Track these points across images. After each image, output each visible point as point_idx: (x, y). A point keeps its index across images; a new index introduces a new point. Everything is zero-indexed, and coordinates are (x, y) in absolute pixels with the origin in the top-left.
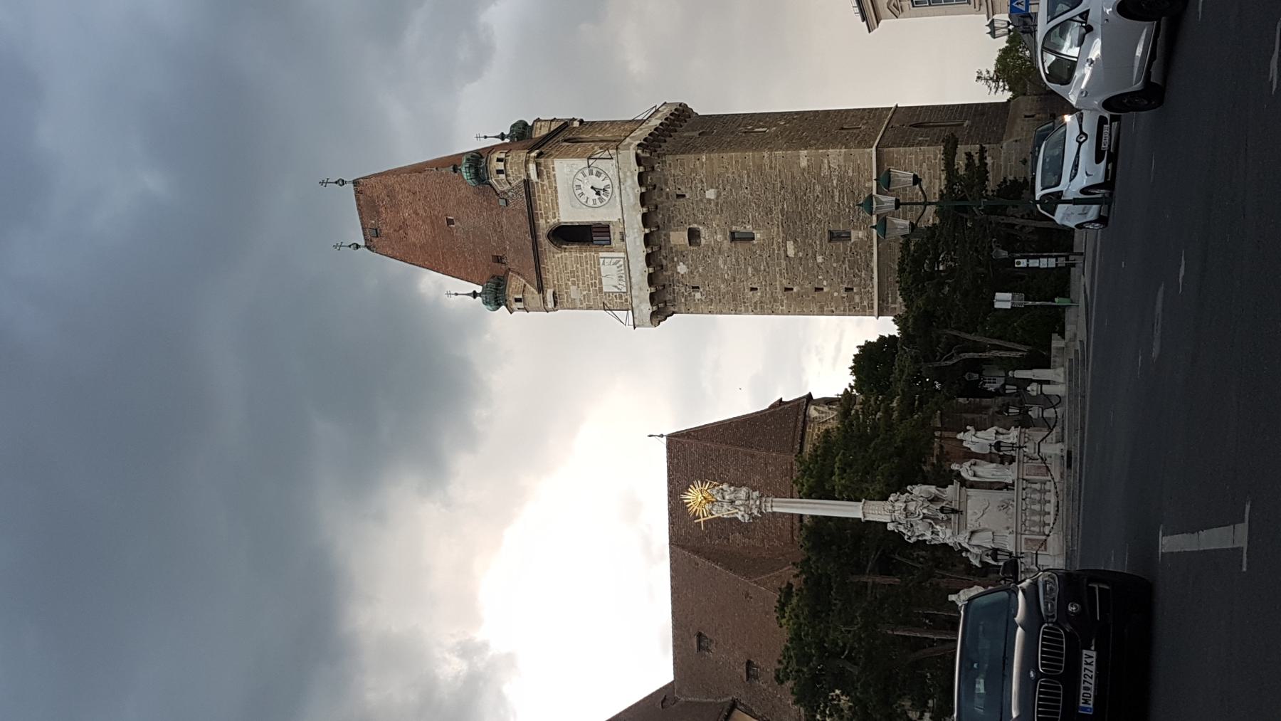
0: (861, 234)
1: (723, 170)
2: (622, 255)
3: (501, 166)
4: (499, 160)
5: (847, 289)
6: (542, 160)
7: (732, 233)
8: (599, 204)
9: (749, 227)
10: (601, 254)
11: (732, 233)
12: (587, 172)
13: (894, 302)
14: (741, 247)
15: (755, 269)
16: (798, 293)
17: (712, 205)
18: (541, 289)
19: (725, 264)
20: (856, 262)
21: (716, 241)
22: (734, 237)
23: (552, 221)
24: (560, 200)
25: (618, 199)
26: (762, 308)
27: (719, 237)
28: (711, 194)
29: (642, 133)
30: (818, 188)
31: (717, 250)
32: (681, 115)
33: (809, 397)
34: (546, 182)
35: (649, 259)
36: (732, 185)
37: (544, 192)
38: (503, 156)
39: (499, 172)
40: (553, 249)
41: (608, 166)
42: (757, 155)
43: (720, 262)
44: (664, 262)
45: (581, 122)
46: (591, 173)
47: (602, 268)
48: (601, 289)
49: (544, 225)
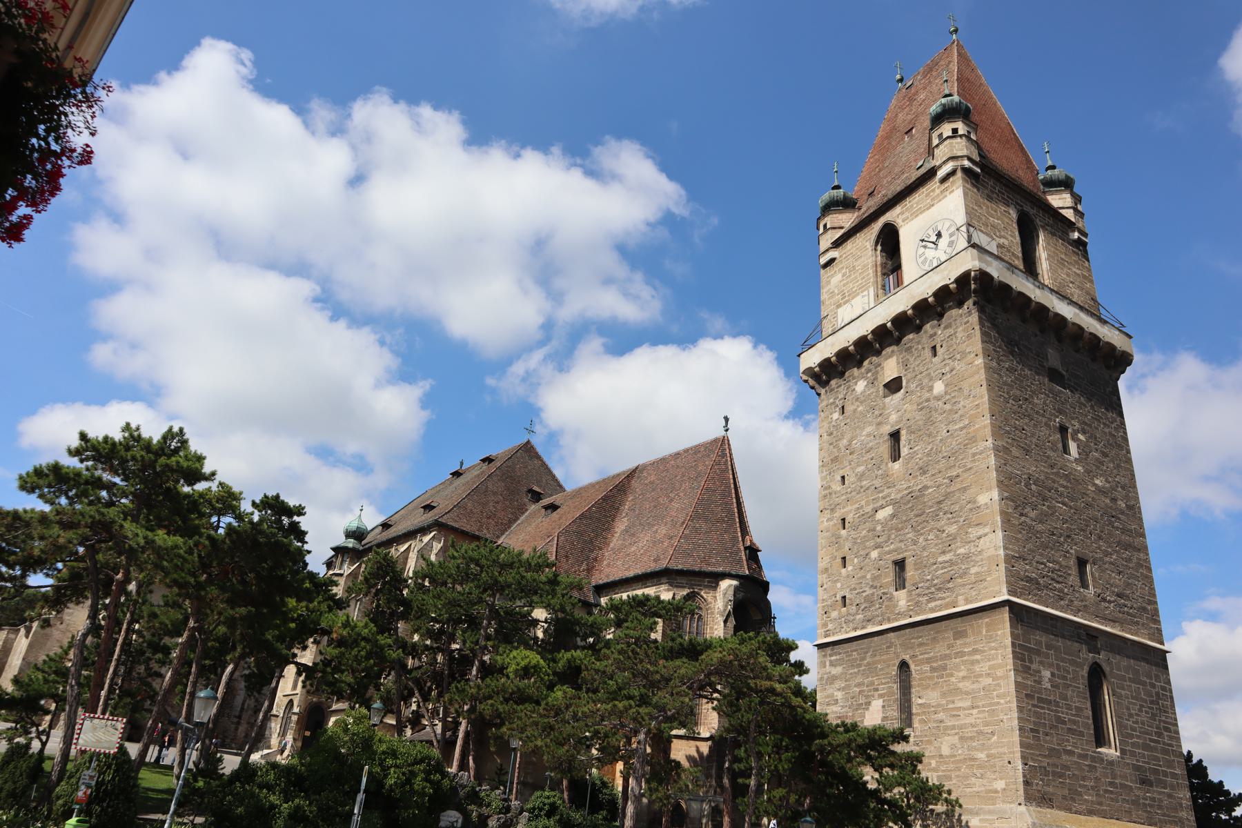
1: (966, 392)
4: (955, 131)
5: (844, 597)
6: (959, 174)
8: (920, 260)
9: (904, 451)
10: (872, 290)
12: (953, 229)
13: (832, 664)
14: (885, 448)
15: (863, 474)
16: (839, 537)
17: (927, 395)
18: (837, 244)
19: (868, 435)
21: (889, 414)
22: (895, 436)
23: (899, 222)
24: (921, 217)
26: (825, 496)
27: (894, 417)
28: (939, 387)
30: (952, 529)
34: (938, 191)
38: (960, 132)
42: (988, 431)
43: (869, 429)
44: (866, 363)
46: (951, 235)
48: (839, 306)
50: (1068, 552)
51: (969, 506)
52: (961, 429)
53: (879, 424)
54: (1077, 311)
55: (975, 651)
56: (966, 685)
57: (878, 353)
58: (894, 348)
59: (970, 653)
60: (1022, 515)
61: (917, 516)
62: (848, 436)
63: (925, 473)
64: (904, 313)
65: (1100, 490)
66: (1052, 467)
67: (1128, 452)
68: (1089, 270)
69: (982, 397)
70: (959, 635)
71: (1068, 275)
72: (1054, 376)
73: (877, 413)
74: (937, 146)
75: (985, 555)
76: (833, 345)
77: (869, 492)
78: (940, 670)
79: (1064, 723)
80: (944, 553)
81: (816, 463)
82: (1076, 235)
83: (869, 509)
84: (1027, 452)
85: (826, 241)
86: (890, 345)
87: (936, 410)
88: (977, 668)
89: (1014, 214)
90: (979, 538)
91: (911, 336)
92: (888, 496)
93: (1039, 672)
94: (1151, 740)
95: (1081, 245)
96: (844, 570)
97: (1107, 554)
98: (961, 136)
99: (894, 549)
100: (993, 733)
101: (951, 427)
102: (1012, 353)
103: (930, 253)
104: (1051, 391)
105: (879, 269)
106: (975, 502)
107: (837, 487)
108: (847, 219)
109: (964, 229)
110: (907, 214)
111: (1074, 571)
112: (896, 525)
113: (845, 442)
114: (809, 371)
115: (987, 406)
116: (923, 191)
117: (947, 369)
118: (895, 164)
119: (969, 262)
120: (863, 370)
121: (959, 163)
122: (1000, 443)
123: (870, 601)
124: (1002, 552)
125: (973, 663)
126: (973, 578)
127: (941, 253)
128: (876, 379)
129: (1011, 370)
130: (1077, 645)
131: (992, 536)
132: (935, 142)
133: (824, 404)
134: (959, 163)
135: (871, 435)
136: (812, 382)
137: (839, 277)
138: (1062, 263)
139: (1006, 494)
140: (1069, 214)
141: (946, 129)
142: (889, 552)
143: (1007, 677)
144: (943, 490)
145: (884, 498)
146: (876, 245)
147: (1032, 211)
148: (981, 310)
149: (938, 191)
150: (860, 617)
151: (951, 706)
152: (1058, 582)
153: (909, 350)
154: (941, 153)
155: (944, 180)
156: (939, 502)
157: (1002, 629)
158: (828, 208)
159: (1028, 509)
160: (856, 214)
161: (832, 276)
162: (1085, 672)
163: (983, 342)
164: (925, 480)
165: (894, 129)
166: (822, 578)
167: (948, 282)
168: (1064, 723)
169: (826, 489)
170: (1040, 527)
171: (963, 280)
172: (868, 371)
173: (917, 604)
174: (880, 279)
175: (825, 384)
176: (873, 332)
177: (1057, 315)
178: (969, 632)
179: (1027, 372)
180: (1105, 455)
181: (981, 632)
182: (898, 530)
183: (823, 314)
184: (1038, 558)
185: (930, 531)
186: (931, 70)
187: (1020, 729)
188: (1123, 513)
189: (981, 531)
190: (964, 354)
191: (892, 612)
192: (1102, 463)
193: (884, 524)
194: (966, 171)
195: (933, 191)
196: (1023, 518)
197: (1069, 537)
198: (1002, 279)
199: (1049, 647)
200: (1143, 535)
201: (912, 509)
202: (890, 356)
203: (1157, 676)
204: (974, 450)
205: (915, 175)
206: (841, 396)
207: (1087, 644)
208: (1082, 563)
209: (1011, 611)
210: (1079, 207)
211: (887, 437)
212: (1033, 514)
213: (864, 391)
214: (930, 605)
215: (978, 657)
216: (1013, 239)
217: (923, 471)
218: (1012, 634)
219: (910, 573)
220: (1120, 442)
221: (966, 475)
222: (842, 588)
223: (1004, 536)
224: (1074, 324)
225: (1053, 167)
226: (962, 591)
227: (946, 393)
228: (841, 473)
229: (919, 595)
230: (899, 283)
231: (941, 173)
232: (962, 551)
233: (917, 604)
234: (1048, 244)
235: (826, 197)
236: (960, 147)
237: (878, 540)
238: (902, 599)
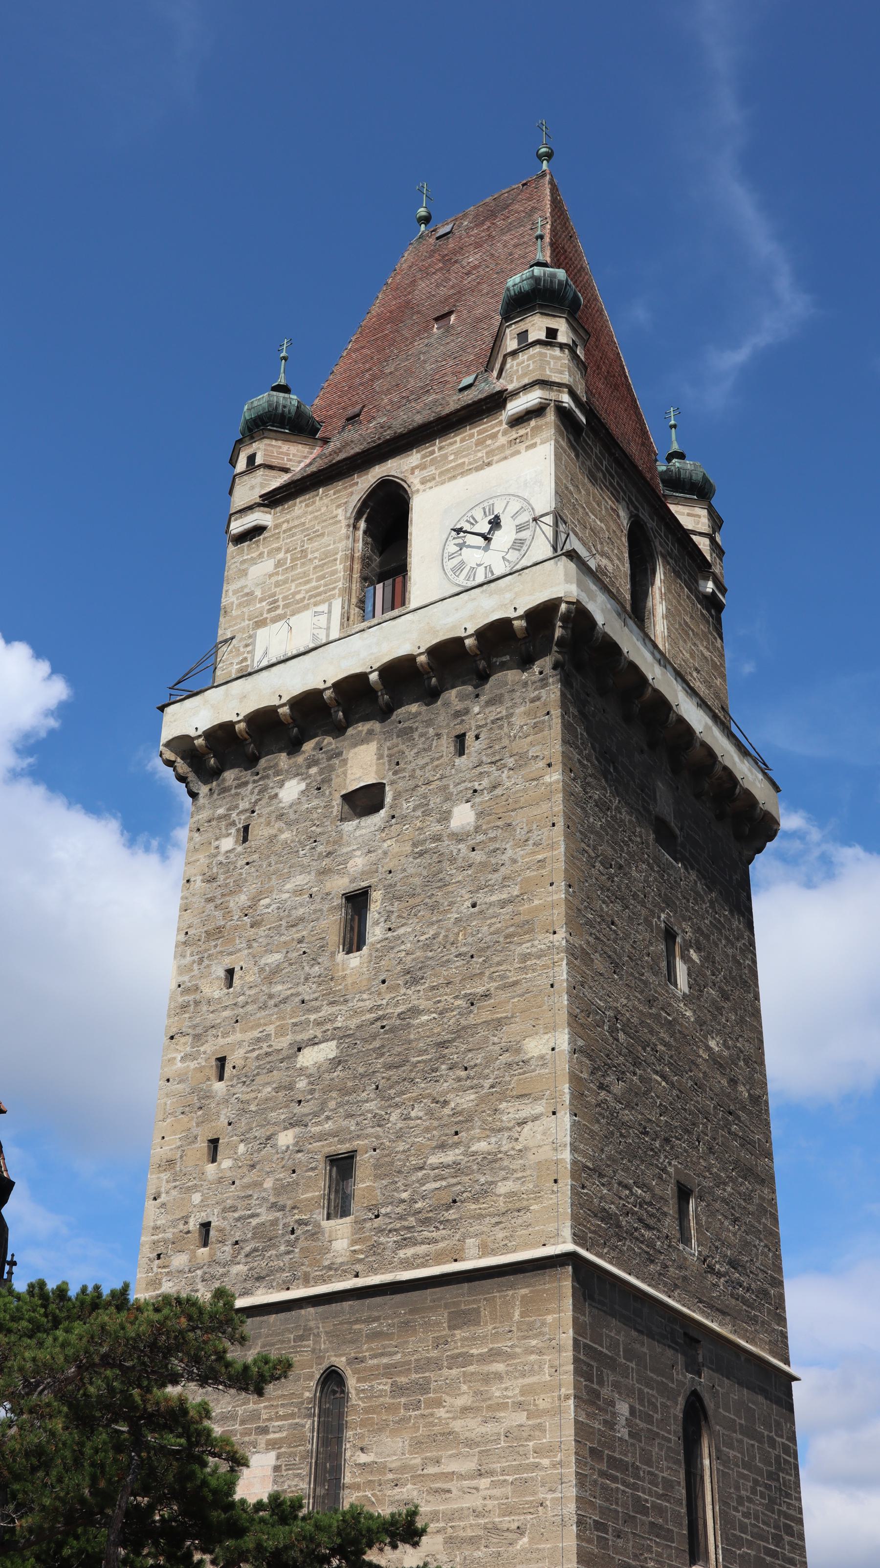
1: (520, 834)
4: (552, 333)
6: (551, 416)
8: (450, 564)
9: (375, 933)
12: (526, 517)
14: (332, 923)
15: (276, 970)
16: (208, 1095)
17: (436, 828)
18: (273, 500)
19: (298, 892)
20: (271, 1241)
21: (350, 856)
22: (357, 902)
23: (414, 482)
24: (461, 482)
26: (184, 1007)
27: (358, 863)
28: (463, 816)
30: (467, 1100)
31: (331, 860)
34: (502, 440)
36: (483, 865)
37: (478, 444)
42: (559, 915)
43: (300, 880)
44: (308, 747)
46: (520, 528)
47: (306, 615)
48: (261, 623)
50: (664, 1170)
51: (506, 1058)
52: (503, 904)
53: (324, 872)
54: (710, 722)
55: (494, 1355)
56: (470, 1427)
57: (339, 730)
58: (375, 725)
59: (483, 1359)
60: (601, 1087)
61: (389, 1067)
62: (251, 888)
63: (415, 981)
64: (410, 659)
65: (716, 1062)
66: (650, 1002)
67: (757, 997)
68: (722, 656)
69: (552, 847)
70: (463, 1318)
71: (692, 655)
72: (664, 835)
73: (321, 848)
74: (514, 353)
75: (532, 1159)
76: (244, 697)
77: (288, 1007)
78: (415, 1391)
79: (644, 1511)
80: (442, 1147)
81: (171, 938)
82: (710, 587)
83: (283, 1043)
84: (617, 967)
85: (249, 490)
86: (366, 718)
87: (453, 860)
88: (496, 1391)
89: (625, 522)
90: (522, 1123)
91: (414, 708)
92: (331, 1019)
93: (612, 1404)
94: (768, 1552)
95: (713, 605)
96: (211, 1168)
97: (720, 1183)
98: (562, 346)
99: (332, 1130)
100: (520, 1531)
101: (481, 898)
102: (605, 774)
103: (473, 556)
104: (657, 860)
105: (357, 566)
106: (518, 1051)
107: (214, 990)
108: (298, 457)
109: (549, 519)
110: (432, 470)
111: (671, 1209)
112: (341, 1082)
113: (243, 899)
114: (183, 746)
115: (561, 865)
116: (471, 434)
117: (485, 782)
118: (409, 372)
119: (558, 583)
120: (300, 759)
121: (552, 395)
122: (577, 941)
123: (265, 1236)
124: (566, 1155)
125: (487, 1379)
126: (501, 1205)
127: (496, 557)
128: (327, 781)
129: (602, 806)
130: (669, 1353)
131: (549, 1122)
132: (511, 344)
133: (204, 815)
134: (552, 395)
135: (303, 892)
136: (182, 767)
137: (268, 565)
138: (684, 629)
139: (581, 1043)
140: (703, 544)
141: (537, 326)
142: (321, 1137)
143: (559, 1411)
144: (451, 1019)
145: (318, 1023)
146: (358, 517)
147: (651, 524)
148: (566, 682)
149: (502, 440)
150: (239, 1269)
151: (431, 1470)
152: (648, 1227)
153: (406, 733)
154: (519, 369)
155: (518, 421)
156: (443, 1045)
157: (557, 1313)
158: (264, 424)
159: (611, 1078)
160: (317, 451)
161: (253, 561)
162: (678, 1410)
163: (565, 742)
164: (416, 997)
165: (405, 308)
166: (156, 1180)
167: (513, 615)
168: (644, 1511)
169: (187, 991)
170: (627, 1115)
171: (542, 615)
172: (312, 762)
173: (374, 1249)
174: (356, 586)
175: (209, 775)
176: (337, 686)
177: (681, 721)
178: (485, 1313)
179: (625, 816)
180: (725, 997)
181: (510, 1316)
182: (344, 1091)
183: (223, 633)
184: (621, 1175)
185: (417, 1100)
186: (492, 214)
187: (579, 1523)
188: (743, 1108)
189: (527, 1110)
190: (523, 759)
191: (315, 1263)
192: (720, 1009)
193: (315, 1077)
194: (563, 413)
195: (494, 436)
196: (603, 1093)
197: (667, 1140)
198: (607, 629)
199: (630, 1354)
200: (769, 1155)
201: (380, 1052)
202: (364, 741)
203: (778, 1424)
204: (525, 948)
205: (454, 402)
206: (244, 805)
207: (684, 1354)
208: (684, 1194)
209: (576, 1277)
210: (718, 539)
211: (338, 901)
212: (618, 1088)
213: (298, 802)
214: (402, 1254)
215: (500, 1367)
216: (618, 566)
217: (413, 977)
218: (575, 1320)
219: (364, 1183)
220: (748, 980)
221: (503, 995)
222: (203, 1205)
223: (574, 1124)
224: (704, 745)
225: (681, 456)
226: (476, 1228)
227: (477, 829)
229: (380, 1231)
230: (397, 600)
231: (515, 407)
232: (482, 1146)
233: (374, 1249)
234: (668, 589)
235: (262, 400)
236: (557, 365)
237: (297, 1109)
238: (340, 1236)
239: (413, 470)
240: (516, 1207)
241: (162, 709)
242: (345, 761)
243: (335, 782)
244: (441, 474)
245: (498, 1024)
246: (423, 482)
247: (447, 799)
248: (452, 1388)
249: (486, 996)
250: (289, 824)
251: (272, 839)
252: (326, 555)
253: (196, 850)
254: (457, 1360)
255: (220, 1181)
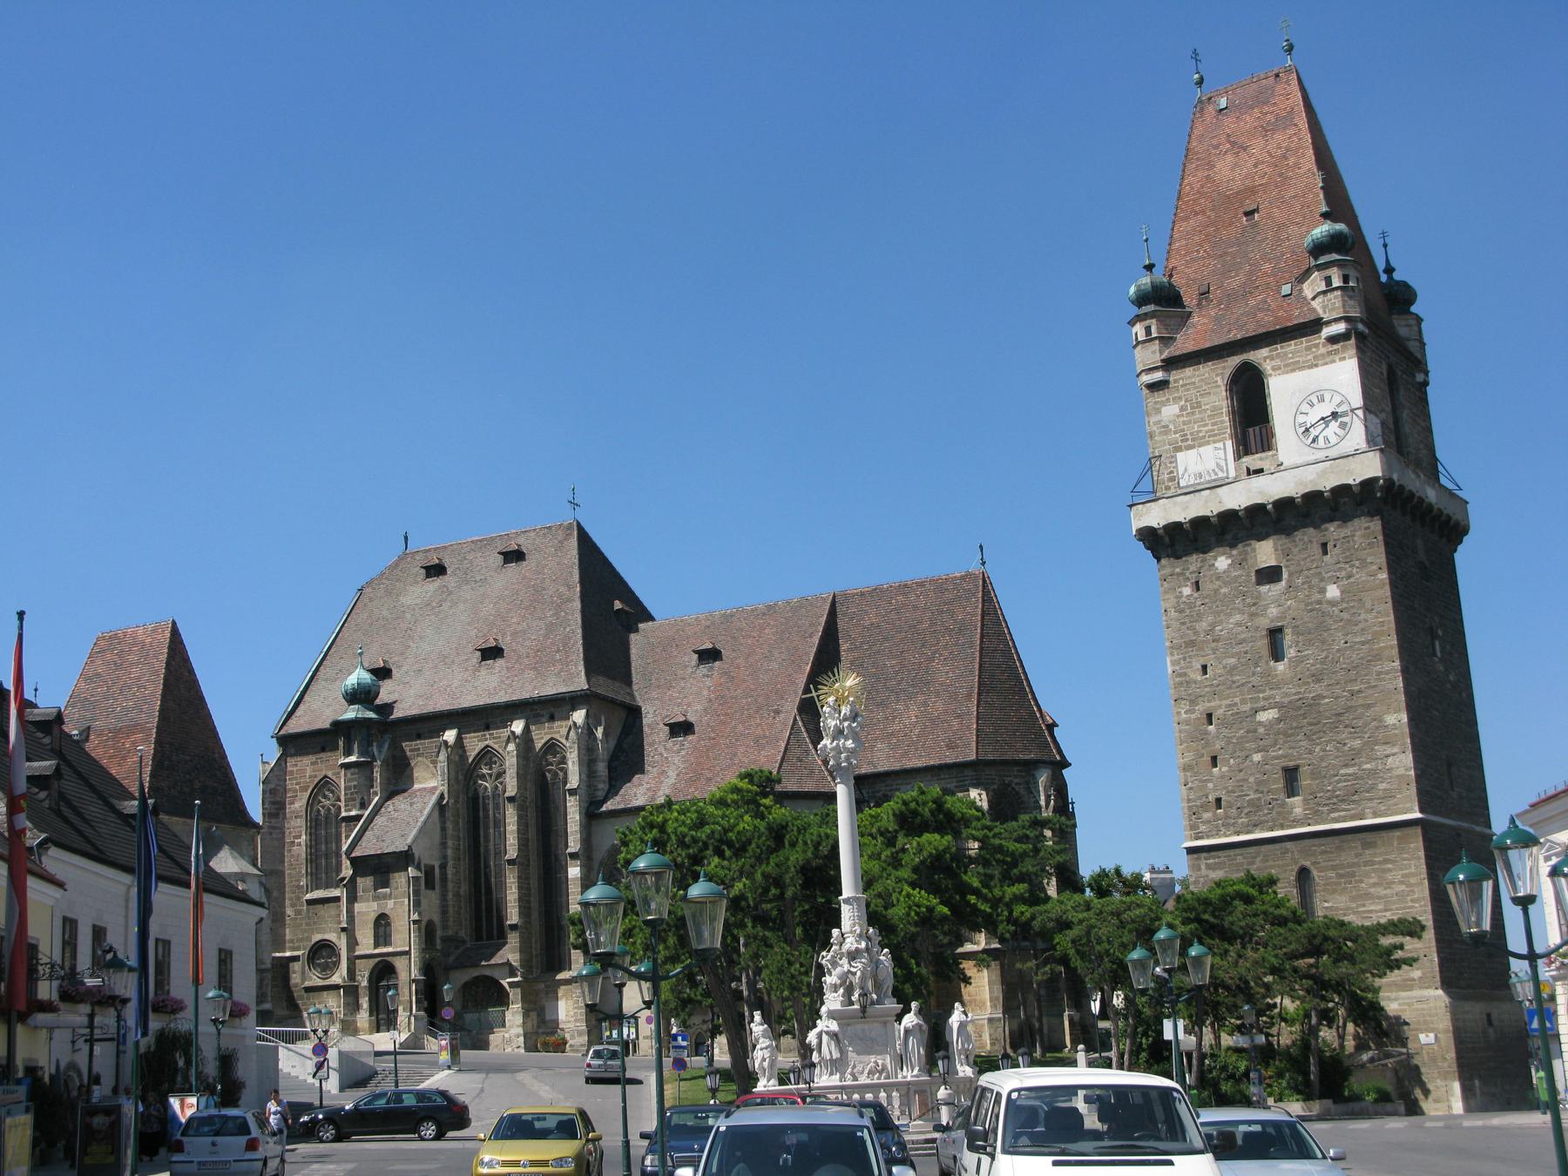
0: (1298, 811)
2: (1232, 474)
3: (1336, 282)
5: (1218, 800)
6: (1353, 341)
7: (1280, 630)
9: (1291, 652)
10: (1229, 443)
11: (1280, 630)
13: (1208, 867)
15: (1234, 668)
16: (1207, 733)
19: (1238, 624)
21: (1266, 607)
22: (1275, 634)
23: (1267, 367)
25: (1312, 458)
27: (1273, 611)
28: (1333, 592)
29: (1413, 482)
30: (1357, 743)
32: (1452, 530)
33: (1065, 764)
34: (1322, 350)
35: (1229, 517)
37: (1308, 349)
39: (1328, 280)
40: (1228, 372)
41: (1357, 436)
42: (1395, 652)
43: (1238, 617)
45: (1426, 384)
47: (1210, 448)
48: (1179, 449)
49: (1259, 356)
52: (1363, 643)
53: (1252, 615)
55: (1386, 861)
59: (1380, 863)
63: (1319, 681)
70: (1366, 845)
74: (1324, 293)
80: (1346, 766)
83: (1246, 707)
88: (1389, 876)
99: (1282, 754)
109: (1360, 413)
110: (1277, 362)
115: (1393, 625)
123: (1255, 805)
125: (1385, 871)
128: (1245, 560)
142: (1277, 758)
145: (1265, 699)
155: (1333, 340)
156: (1339, 714)
161: (1164, 404)
164: (1318, 689)
169: (1180, 675)
171: (1368, 484)
201: (1304, 716)
206: (1193, 568)
208: (1450, 765)
219: (1305, 781)
222: (1215, 789)
227: (1342, 600)
228: (1202, 661)
239: (1265, 359)
240: (1388, 795)
241: (1130, 506)
242: (1254, 550)
243: (1250, 561)
244: (1286, 366)
245: (1369, 706)
246: (1274, 369)
247: (1322, 580)
248: (1367, 875)
249: (1360, 691)
250: (1226, 584)
251: (1216, 591)
252: (1214, 409)
253: (1166, 592)
254: (1366, 863)
255: (1222, 777)
